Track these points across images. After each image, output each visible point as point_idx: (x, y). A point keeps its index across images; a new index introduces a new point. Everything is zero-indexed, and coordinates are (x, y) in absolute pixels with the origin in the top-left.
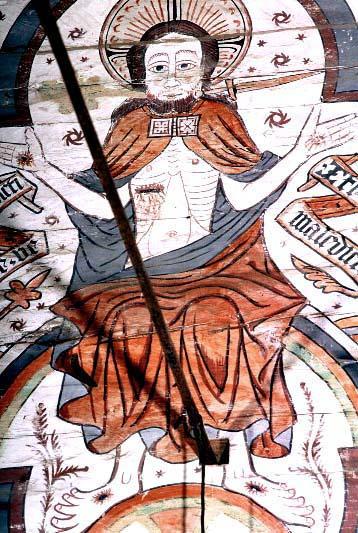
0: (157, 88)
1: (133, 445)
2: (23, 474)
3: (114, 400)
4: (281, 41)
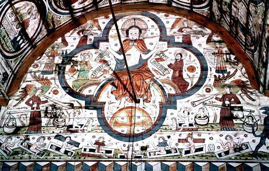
0: (131, 37)
1: (123, 99)
2: (105, 103)
3: (121, 91)
4: (153, 30)
